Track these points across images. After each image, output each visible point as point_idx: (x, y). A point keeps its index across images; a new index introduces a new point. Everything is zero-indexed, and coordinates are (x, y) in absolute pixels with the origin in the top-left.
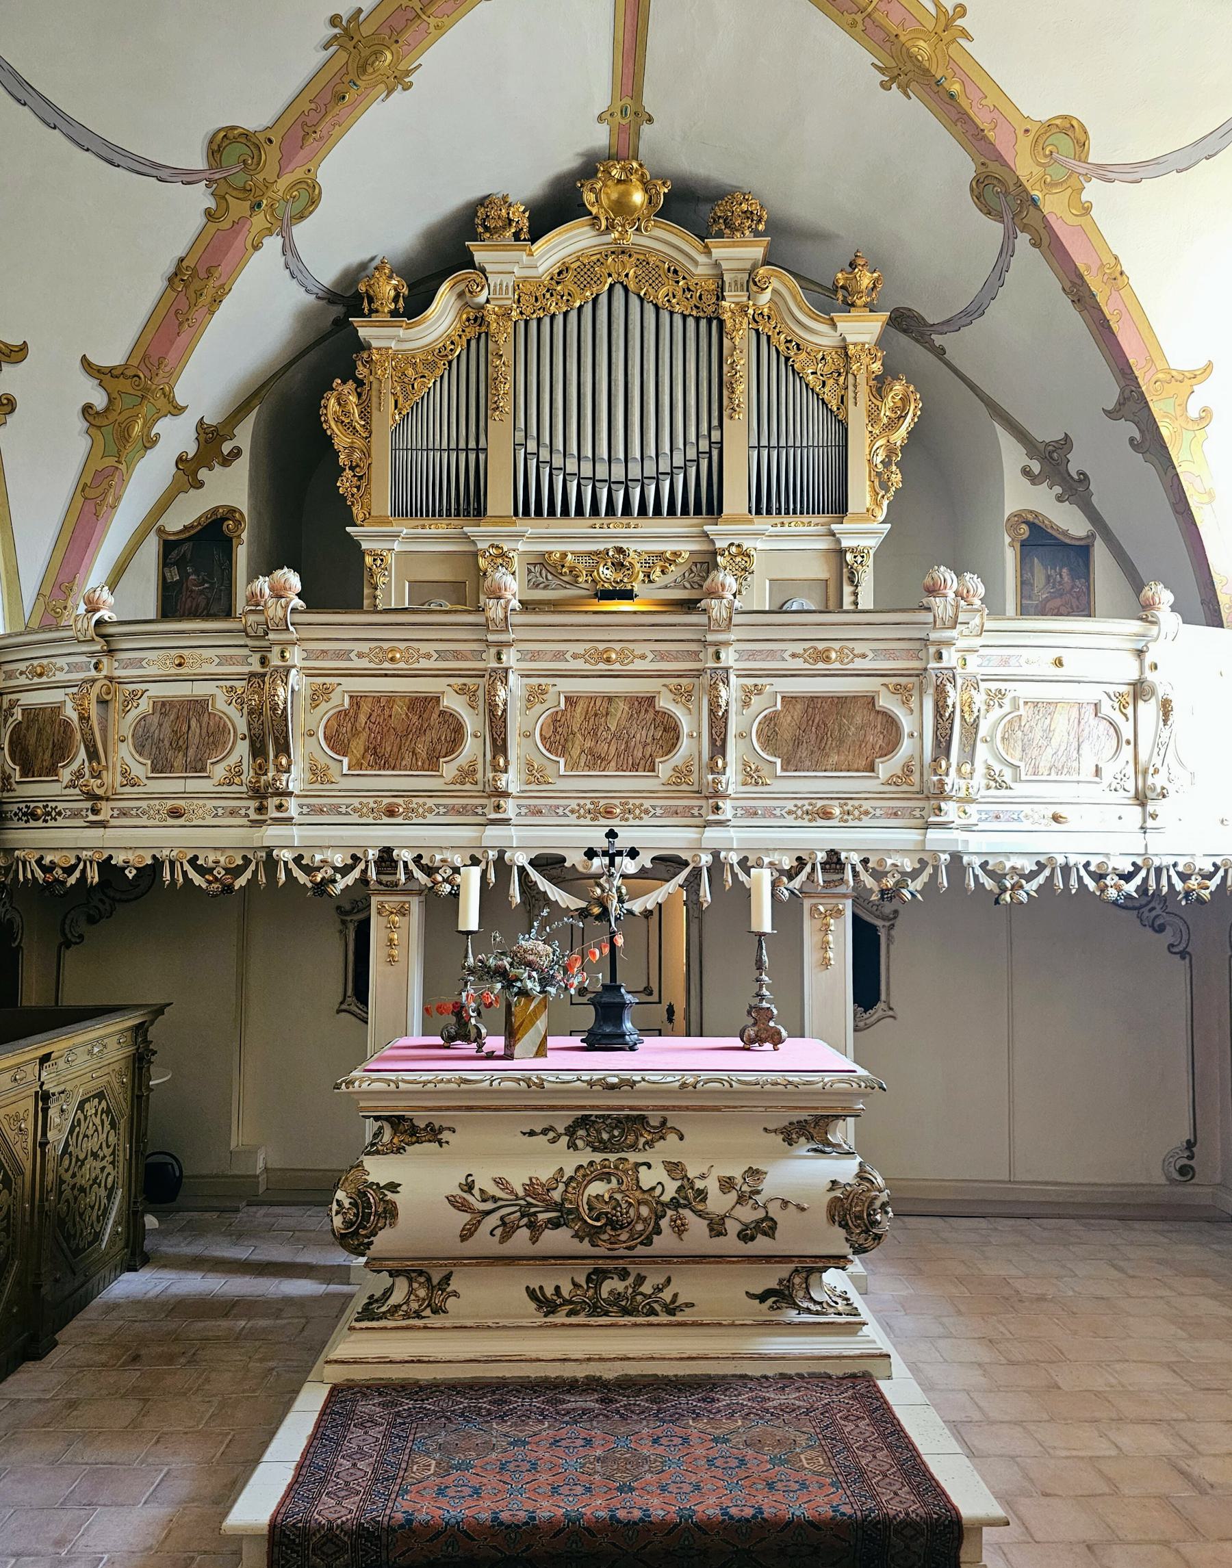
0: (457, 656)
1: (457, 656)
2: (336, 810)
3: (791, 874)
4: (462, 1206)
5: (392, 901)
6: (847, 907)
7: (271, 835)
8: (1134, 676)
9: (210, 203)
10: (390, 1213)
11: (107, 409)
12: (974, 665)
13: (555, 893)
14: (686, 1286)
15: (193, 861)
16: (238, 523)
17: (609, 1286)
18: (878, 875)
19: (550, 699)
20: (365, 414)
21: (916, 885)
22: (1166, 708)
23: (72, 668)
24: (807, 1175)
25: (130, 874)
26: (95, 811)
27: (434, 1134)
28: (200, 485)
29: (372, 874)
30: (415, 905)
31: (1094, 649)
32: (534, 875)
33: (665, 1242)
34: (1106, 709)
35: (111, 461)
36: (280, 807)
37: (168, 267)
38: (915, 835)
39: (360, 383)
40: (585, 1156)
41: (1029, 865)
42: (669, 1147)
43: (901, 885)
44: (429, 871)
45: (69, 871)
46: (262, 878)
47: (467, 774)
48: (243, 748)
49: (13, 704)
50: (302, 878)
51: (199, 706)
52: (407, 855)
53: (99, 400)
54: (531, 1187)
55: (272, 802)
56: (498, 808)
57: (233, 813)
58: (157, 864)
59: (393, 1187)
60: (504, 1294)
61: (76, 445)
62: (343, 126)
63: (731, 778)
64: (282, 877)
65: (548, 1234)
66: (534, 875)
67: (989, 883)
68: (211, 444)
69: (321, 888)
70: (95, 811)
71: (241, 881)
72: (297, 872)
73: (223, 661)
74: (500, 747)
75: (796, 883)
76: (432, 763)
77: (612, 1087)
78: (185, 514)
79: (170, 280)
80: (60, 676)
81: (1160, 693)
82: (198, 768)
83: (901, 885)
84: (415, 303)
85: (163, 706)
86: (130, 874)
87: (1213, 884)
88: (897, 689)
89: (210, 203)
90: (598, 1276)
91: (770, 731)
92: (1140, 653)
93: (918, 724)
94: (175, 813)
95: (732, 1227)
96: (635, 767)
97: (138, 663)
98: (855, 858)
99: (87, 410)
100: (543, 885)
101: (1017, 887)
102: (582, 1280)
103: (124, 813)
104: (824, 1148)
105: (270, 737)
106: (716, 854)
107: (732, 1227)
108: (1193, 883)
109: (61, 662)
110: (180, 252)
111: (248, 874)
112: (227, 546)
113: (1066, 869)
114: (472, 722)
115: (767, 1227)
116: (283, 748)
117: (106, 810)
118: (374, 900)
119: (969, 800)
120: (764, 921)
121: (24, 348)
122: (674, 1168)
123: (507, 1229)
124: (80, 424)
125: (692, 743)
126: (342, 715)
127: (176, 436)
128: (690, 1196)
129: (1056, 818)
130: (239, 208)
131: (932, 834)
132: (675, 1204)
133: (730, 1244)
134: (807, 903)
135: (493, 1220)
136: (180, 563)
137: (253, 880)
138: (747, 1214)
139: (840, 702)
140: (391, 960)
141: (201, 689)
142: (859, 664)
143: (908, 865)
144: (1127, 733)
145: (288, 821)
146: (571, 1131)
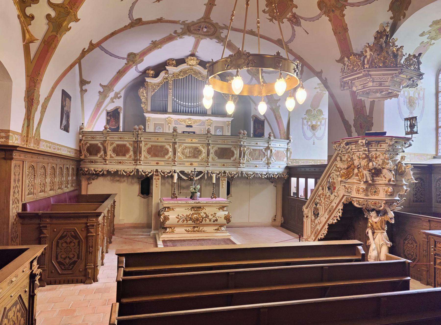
0: (168, 139)
1: (168, 139)
2: (148, 163)
3: (219, 174)
4: (178, 218)
5: (157, 177)
6: (226, 179)
7: (138, 167)
8: (267, 146)
9: (126, 62)
10: (168, 219)
11: (103, 92)
12: (245, 144)
13: (183, 177)
14: (205, 229)
15: (124, 171)
16: (121, 109)
17: (196, 229)
18: (231, 174)
19: (183, 146)
20: (147, 93)
21: (236, 176)
22: (271, 151)
23: (100, 138)
24: (222, 214)
25: (112, 172)
26: (105, 162)
27: (173, 209)
28: (114, 102)
29: (154, 173)
30: (160, 178)
31: (261, 144)
32: (180, 174)
33: (204, 222)
34: (263, 151)
35: (102, 100)
36: (140, 162)
37: (117, 71)
38: (236, 169)
39: (145, 88)
40: (193, 212)
41: (252, 173)
42: (204, 211)
43: (234, 176)
44: (164, 173)
45: (101, 171)
46: (136, 174)
47: (170, 157)
48: (131, 153)
49: (87, 143)
50: (143, 174)
51: (124, 146)
52: (160, 170)
53: (102, 90)
54: (187, 216)
55: (138, 162)
56: (174, 163)
57: (130, 163)
58: (117, 171)
59: (169, 216)
60: (182, 230)
61: (96, 98)
62: (150, 53)
63: (210, 159)
64: (140, 174)
65: (189, 222)
66: (180, 174)
67: (246, 176)
68: (117, 96)
69: (146, 175)
70: (105, 162)
71: (132, 174)
72: (142, 173)
73: (129, 138)
74: (175, 154)
75: (219, 176)
76: (164, 157)
77: (197, 203)
78: (111, 107)
79: (117, 73)
80: (98, 139)
81: (271, 148)
82: (124, 155)
83: (234, 176)
84: (156, 75)
85: (118, 145)
86: (112, 172)
87: (277, 176)
88: (235, 147)
89: (126, 62)
90: (194, 227)
91: (216, 152)
92: (268, 142)
93: (237, 153)
94: (120, 163)
95: (212, 220)
96: (195, 157)
97: (113, 138)
98: (228, 172)
99: (99, 92)
100: (181, 175)
101: (250, 176)
102: (192, 228)
103: (111, 162)
104: (224, 211)
105: (137, 151)
106: (208, 171)
107: (212, 220)
108: (274, 176)
109: (98, 137)
110: (120, 69)
111: (133, 173)
112: (119, 113)
113: (257, 174)
114: (170, 150)
115: (217, 220)
116: (140, 153)
117: (107, 161)
118: (154, 177)
119: (244, 164)
120: (214, 181)
121: (90, 82)
122: (205, 213)
123: (183, 221)
124: (98, 94)
125: (204, 155)
126: (149, 148)
127: (112, 95)
128: (207, 216)
129: (256, 166)
130: (131, 63)
131: (239, 169)
132: (205, 217)
133: (212, 222)
134: (221, 179)
135: (182, 220)
136: (110, 116)
137: (134, 174)
138: (214, 219)
139: (226, 149)
140: (157, 187)
141: (125, 143)
142: (229, 143)
143: (235, 173)
144: (266, 154)
145: (141, 165)
146: (191, 209)
